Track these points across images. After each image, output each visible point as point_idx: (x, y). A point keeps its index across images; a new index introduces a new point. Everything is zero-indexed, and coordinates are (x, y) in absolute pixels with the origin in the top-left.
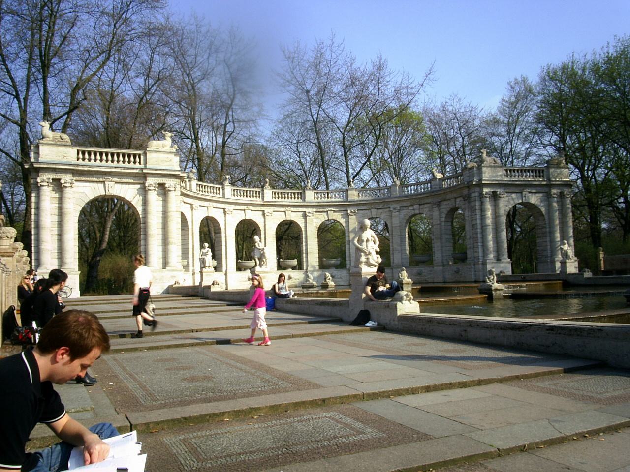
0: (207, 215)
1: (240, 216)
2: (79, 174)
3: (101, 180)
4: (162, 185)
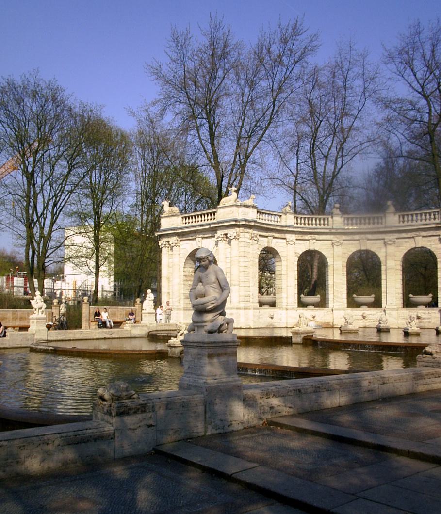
0: (359, 248)
1: (407, 245)
2: (183, 235)
3: (194, 237)
4: (226, 235)
